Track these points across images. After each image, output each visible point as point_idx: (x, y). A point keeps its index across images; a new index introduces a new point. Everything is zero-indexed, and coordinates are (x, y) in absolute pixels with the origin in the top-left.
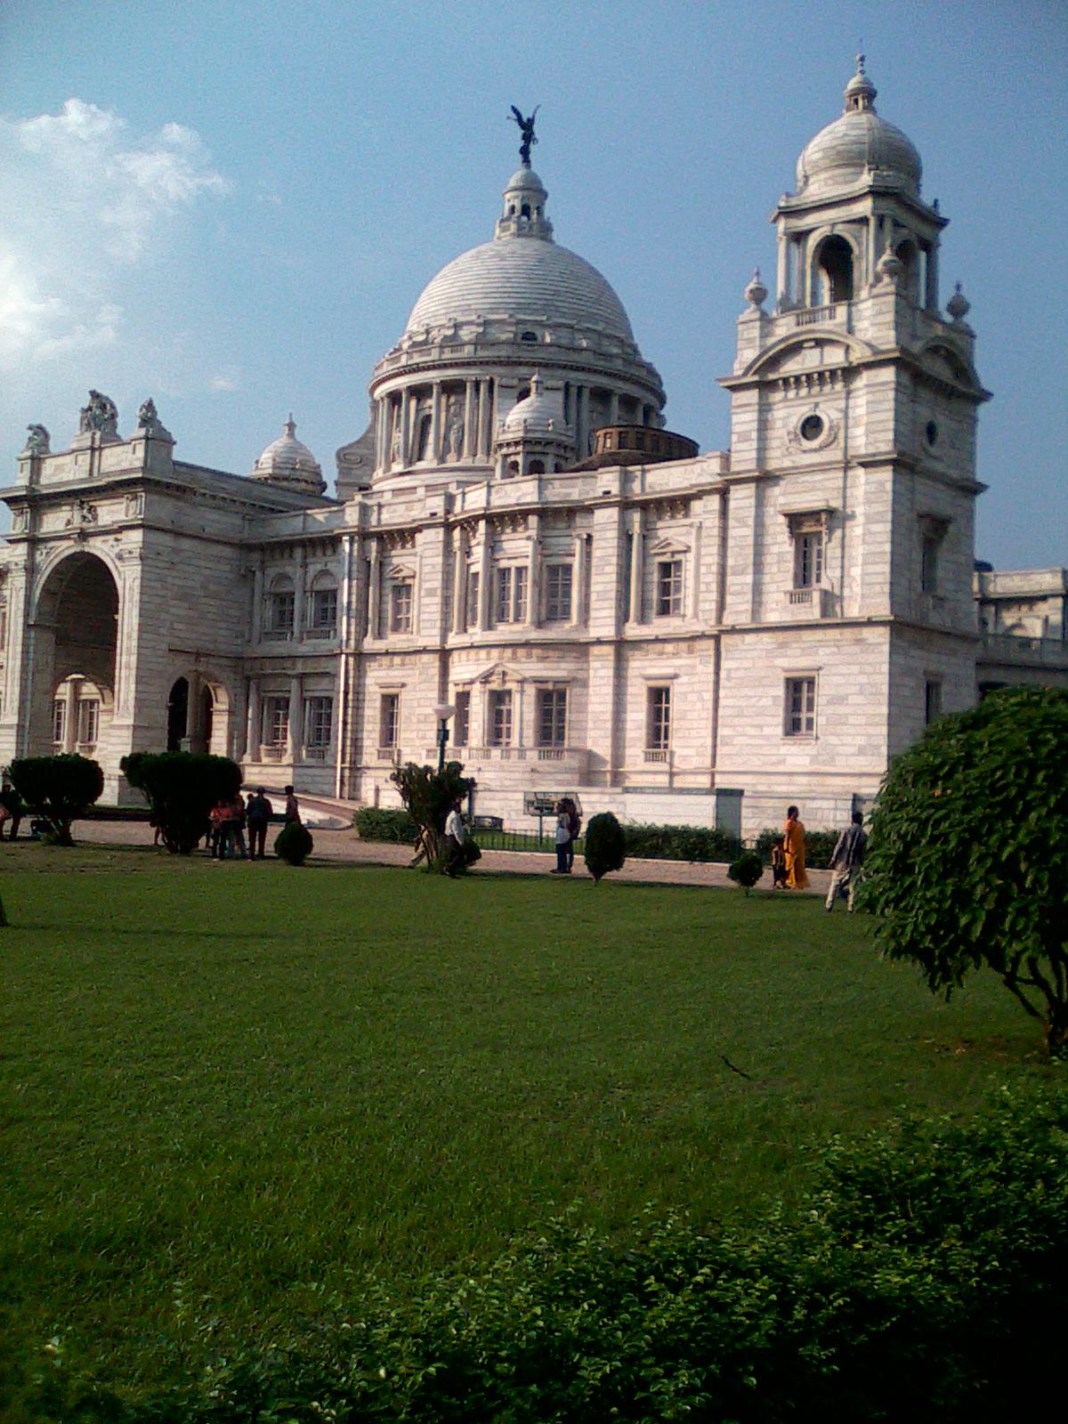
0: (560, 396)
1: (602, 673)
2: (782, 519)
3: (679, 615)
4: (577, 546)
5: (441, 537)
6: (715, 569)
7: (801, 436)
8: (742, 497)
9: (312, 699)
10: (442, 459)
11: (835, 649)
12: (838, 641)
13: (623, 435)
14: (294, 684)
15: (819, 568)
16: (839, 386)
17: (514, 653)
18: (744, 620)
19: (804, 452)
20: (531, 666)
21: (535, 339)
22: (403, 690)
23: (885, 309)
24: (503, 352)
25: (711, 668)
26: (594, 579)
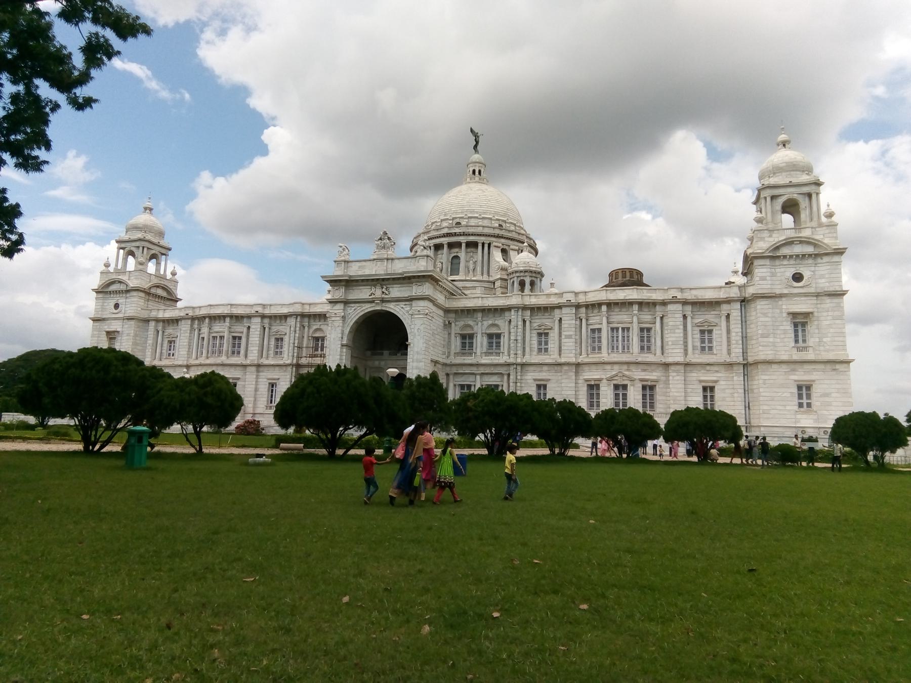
1: (678, 378)
2: (785, 315)
3: (713, 354)
4: (658, 320)
5: (574, 312)
6: (740, 334)
12: (824, 369)
13: (624, 272)
14: (478, 377)
15: (804, 336)
16: (810, 261)
17: (628, 367)
18: (770, 358)
19: (795, 287)
21: (503, 227)
22: (549, 382)
24: (497, 232)
26: (665, 336)
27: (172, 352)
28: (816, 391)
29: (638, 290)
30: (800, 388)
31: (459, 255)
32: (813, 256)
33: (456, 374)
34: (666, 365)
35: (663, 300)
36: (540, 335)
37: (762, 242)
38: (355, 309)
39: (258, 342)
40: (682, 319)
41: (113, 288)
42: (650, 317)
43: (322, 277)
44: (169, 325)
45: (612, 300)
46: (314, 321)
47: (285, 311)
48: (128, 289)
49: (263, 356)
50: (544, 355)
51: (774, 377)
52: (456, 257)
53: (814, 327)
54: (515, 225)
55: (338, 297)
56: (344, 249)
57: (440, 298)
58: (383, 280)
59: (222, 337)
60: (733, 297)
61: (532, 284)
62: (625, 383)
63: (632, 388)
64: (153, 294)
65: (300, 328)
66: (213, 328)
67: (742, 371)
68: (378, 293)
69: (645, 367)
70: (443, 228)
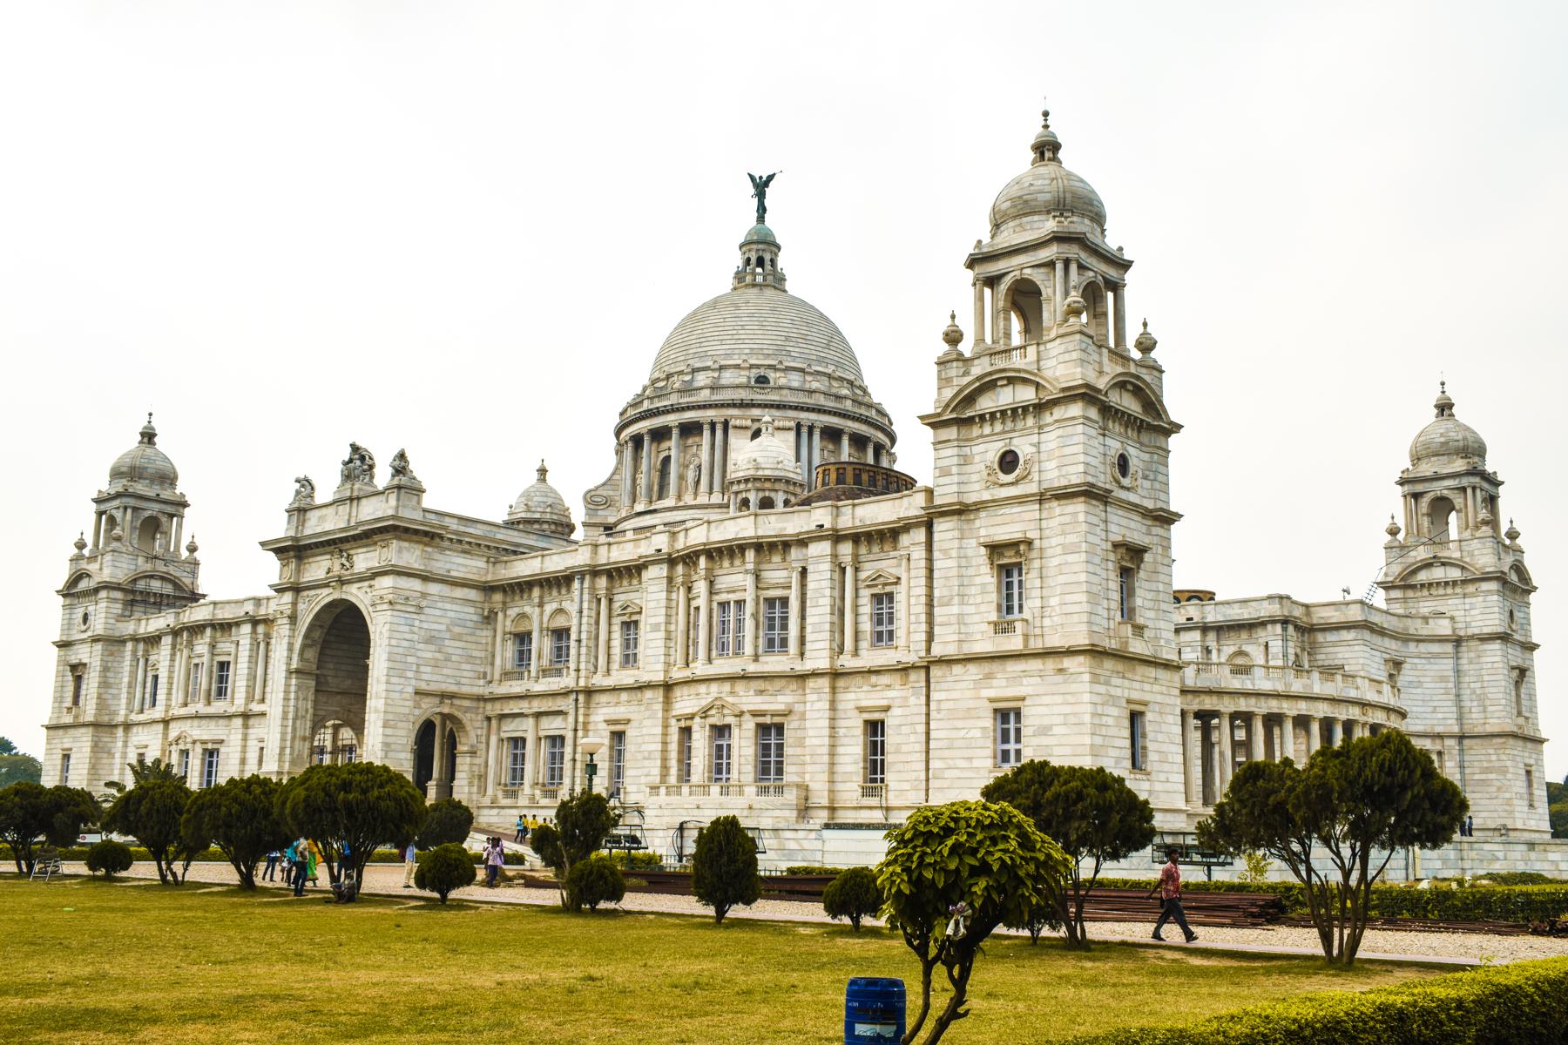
0: (791, 436)
1: (819, 705)
6: (923, 600)
7: (998, 470)
9: (547, 737)
10: (679, 497)
11: (1039, 679)
14: (531, 721)
16: (1030, 421)
17: (732, 686)
19: (1002, 485)
20: (750, 699)
23: (1071, 347)
25: (923, 700)
26: (809, 611)
28: (1032, 718)
33: (502, 717)
34: (803, 677)
41: (83, 585)
42: (784, 574)
43: (263, 544)
49: (257, 697)
51: (954, 695)
52: (667, 460)
53: (1034, 574)
54: (802, 370)
60: (908, 518)
67: (924, 684)
69: (760, 684)
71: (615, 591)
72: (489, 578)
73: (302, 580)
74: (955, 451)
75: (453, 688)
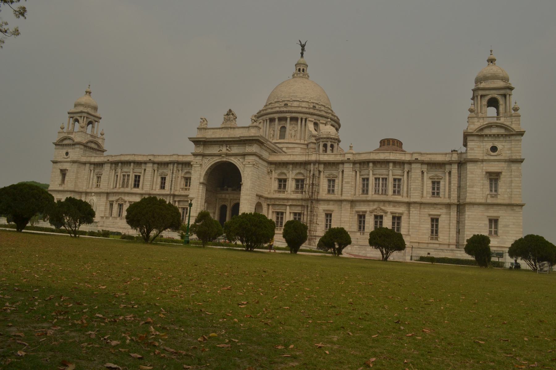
1: (415, 212)
2: (484, 173)
3: (439, 197)
4: (406, 174)
5: (352, 166)
6: (456, 185)
7: (490, 151)
8: (470, 167)
14: (288, 207)
16: (501, 139)
17: (384, 204)
18: (473, 201)
20: (390, 208)
24: (311, 111)
27: (99, 184)
29: (393, 154)
30: (490, 221)
31: (285, 125)
32: (504, 135)
33: (273, 205)
35: (409, 161)
36: (329, 181)
37: (473, 125)
38: (209, 160)
39: (150, 179)
40: (420, 174)
41: (66, 142)
42: (400, 171)
43: (189, 138)
44: (97, 167)
45: (376, 159)
46: (185, 167)
47: (167, 159)
48: (74, 143)
50: (332, 194)
54: (324, 106)
55: (198, 152)
56: (204, 121)
57: (265, 154)
58: (227, 141)
59: (128, 176)
60: (453, 161)
61: (332, 146)
62: (382, 214)
63: (386, 217)
64: (89, 147)
65: (176, 171)
66: (123, 169)
68: (224, 150)
70: (276, 107)
71: (325, 169)
72: (270, 159)
73: (206, 153)
74: (476, 144)
75: (261, 194)
